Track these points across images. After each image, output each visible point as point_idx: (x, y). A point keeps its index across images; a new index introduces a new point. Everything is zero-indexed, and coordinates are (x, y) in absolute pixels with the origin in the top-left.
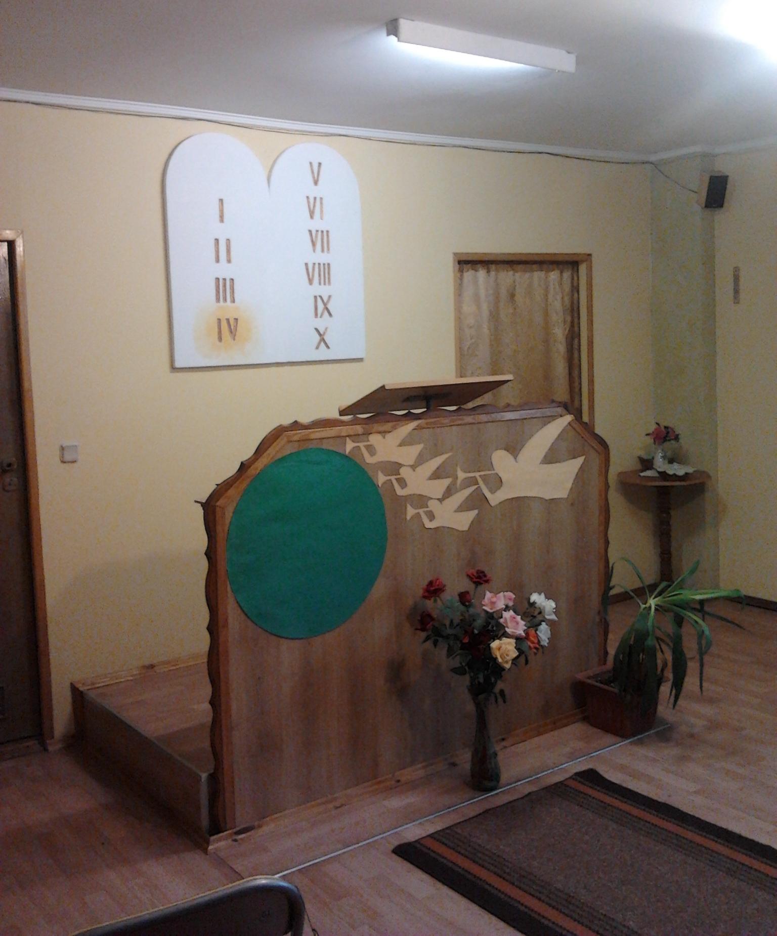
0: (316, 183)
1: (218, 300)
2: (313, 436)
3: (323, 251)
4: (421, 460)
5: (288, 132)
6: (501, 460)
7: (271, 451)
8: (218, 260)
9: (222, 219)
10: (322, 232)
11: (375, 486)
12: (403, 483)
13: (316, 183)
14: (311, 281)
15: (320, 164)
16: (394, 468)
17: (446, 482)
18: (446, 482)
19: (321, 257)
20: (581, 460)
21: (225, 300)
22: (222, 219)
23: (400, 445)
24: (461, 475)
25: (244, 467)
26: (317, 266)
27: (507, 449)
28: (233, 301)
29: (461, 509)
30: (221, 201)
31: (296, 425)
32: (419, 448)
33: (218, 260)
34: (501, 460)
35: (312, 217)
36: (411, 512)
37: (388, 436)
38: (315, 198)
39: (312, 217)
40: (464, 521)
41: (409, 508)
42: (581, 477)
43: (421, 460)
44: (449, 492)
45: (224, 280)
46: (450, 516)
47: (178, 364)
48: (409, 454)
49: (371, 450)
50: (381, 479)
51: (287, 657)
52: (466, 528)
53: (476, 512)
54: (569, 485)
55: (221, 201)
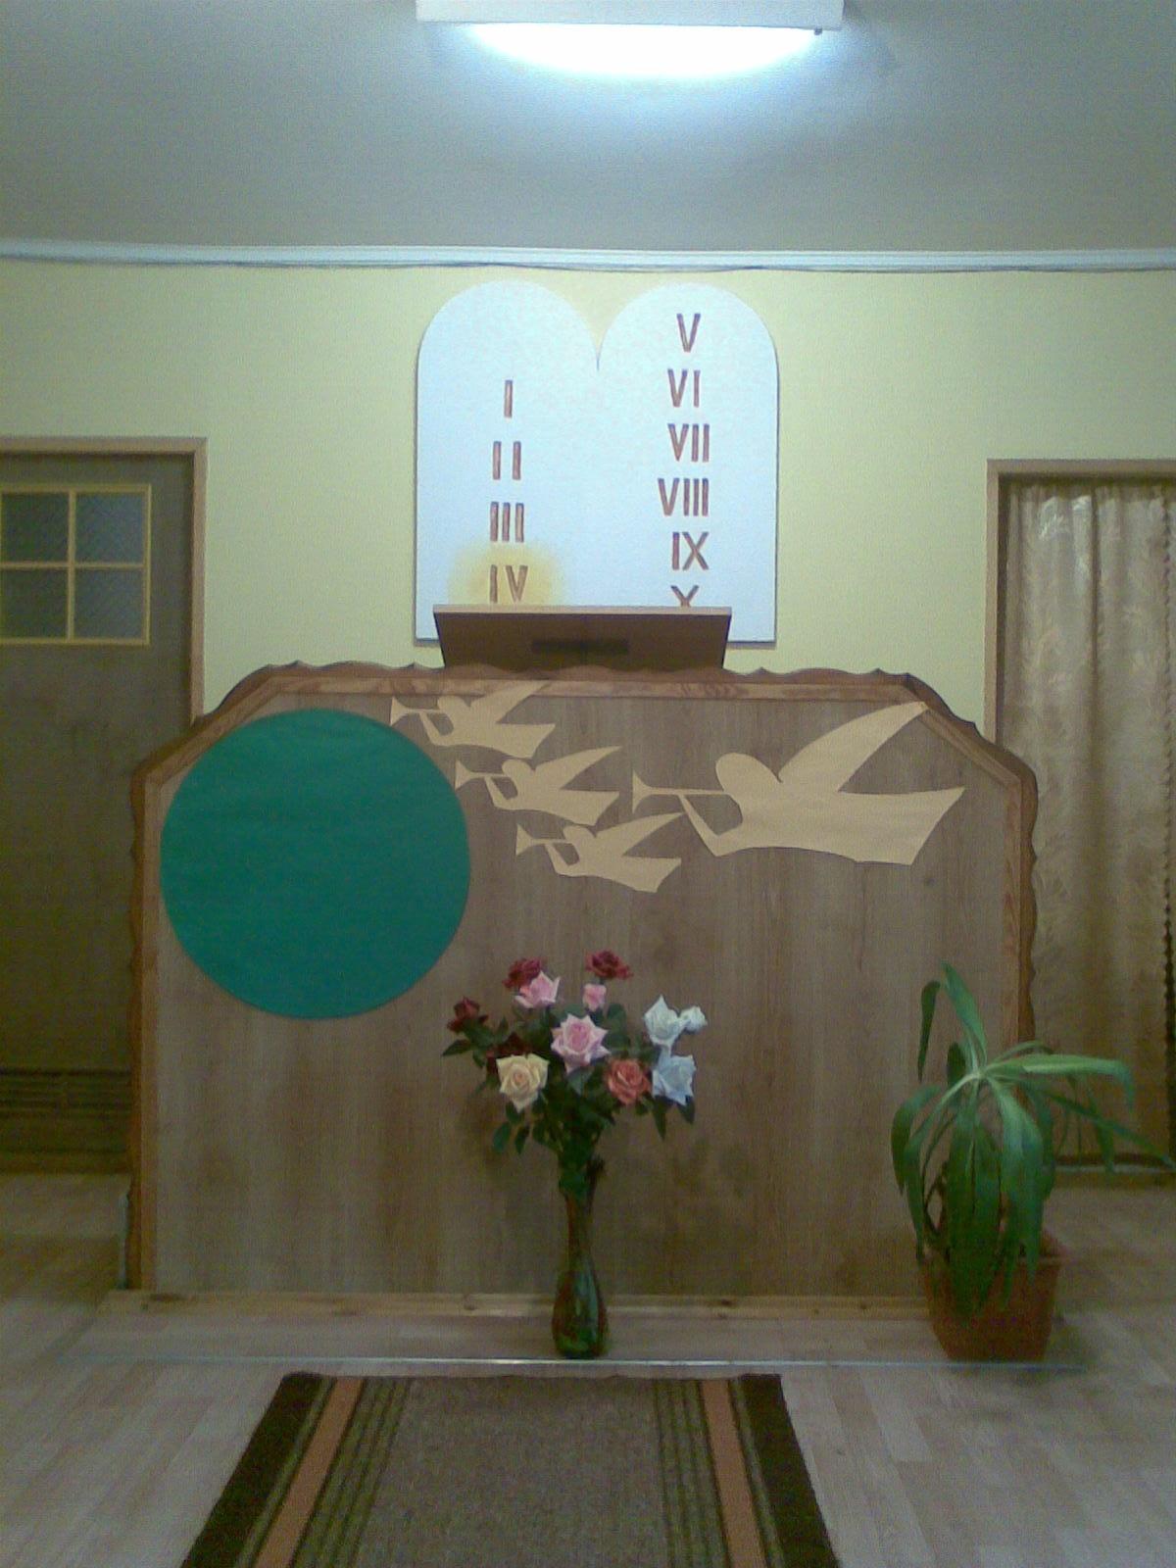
0: (688, 347)
1: (494, 537)
2: (324, 688)
3: (695, 458)
4: (547, 753)
5: (626, 269)
6: (738, 774)
7: (248, 703)
8: (497, 475)
9: (509, 412)
10: (696, 427)
11: (448, 786)
12: (508, 788)
13: (688, 347)
14: (668, 510)
15: (697, 317)
16: (493, 760)
17: (609, 798)
18: (609, 798)
19: (688, 468)
21: (506, 537)
22: (509, 412)
23: (504, 721)
24: (641, 790)
26: (681, 485)
27: (756, 754)
28: (521, 538)
29: (639, 851)
30: (509, 384)
31: (295, 669)
32: (542, 731)
33: (497, 475)
34: (738, 774)
35: (676, 403)
36: (524, 841)
38: (685, 374)
39: (676, 403)
40: (649, 875)
41: (520, 831)
42: (948, 828)
43: (547, 753)
44: (612, 818)
45: (507, 505)
46: (618, 859)
48: (528, 738)
49: (443, 724)
50: (462, 776)
53: (676, 862)
54: (920, 841)
55: (509, 384)
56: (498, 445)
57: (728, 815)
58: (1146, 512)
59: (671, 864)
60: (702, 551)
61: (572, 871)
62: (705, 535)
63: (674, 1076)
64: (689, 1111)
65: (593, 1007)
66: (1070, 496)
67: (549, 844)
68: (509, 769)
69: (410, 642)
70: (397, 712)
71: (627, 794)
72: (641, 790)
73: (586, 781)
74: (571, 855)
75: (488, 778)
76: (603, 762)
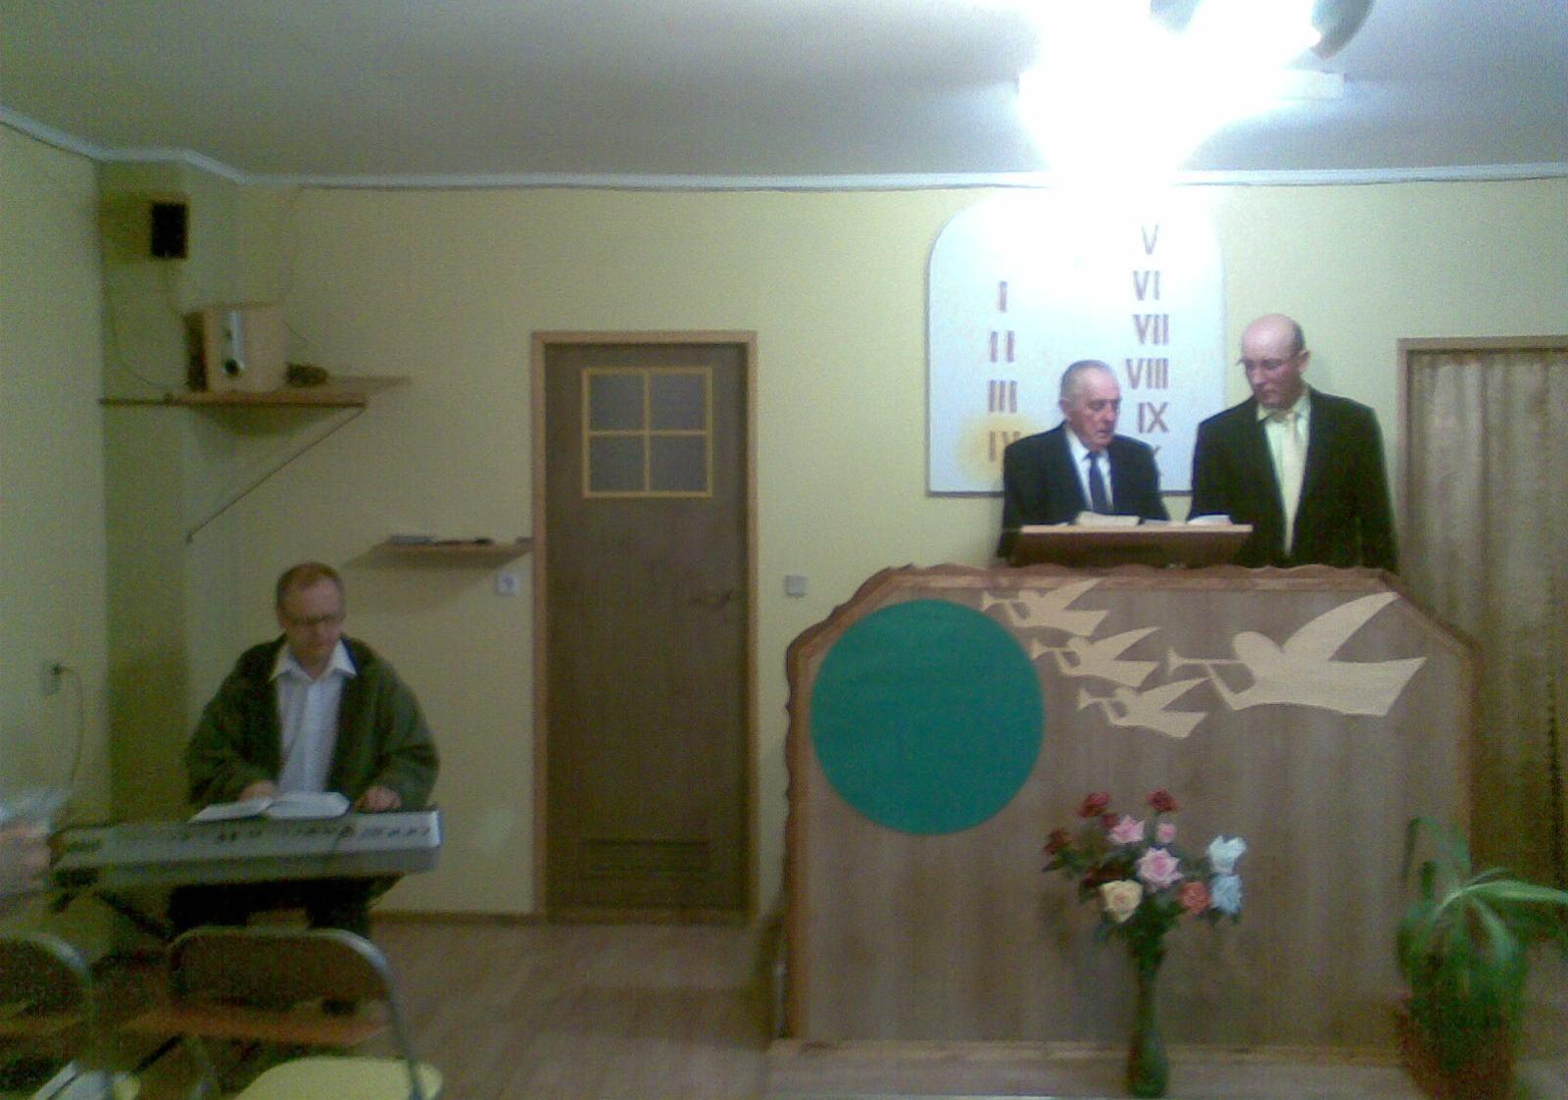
0: (1149, 250)
1: (991, 408)
2: (933, 584)
3: (1156, 342)
4: (1101, 633)
6: (1250, 648)
8: (994, 358)
9: (1003, 306)
13: (1149, 250)
16: (1059, 638)
17: (1148, 667)
18: (1148, 667)
19: (1151, 351)
20: (1415, 664)
21: (1001, 408)
22: (1003, 306)
25: (838, 613)
26: (1145, 365)
27: (1265, 631)
28: (1013, 409)
29: (1175, 706)
30: (1003, 285)
31: (907, 569)
32: (1098, 616)
33: (994, 358)
36: (1085, 700)
37: (1049, 595)
40: (1182, 725)
42: (1412, 689)
43: (1101, 633)
44: (1152, 681)
46: (1157, 713)
47: (935, 487)
48: (1087, 621)
49: (1022, 611)
50: (1037, 650)
51: (888, 851)
52: (1184, 735)
54: (1390, 699)
56: (994, 335)
57: (1242, 679)
58: (1526, 376)
59: (1199, 717)
60: (1164, 417)
61: (1123, 722)
62: (1164, 406)
63: (1227, 893)
64: (1235, 918)
65: (1167, 840)
66: (1461, 363)
67: (1104, 701)
68: (1073, 645)
69: (923, 491)
70: (988, 601)
71: (1164, 663)
72: (1175, 661)
73: (1132, 654)
74: (1121, 710)
75: (1057, 651)
76: (1146, 639)
